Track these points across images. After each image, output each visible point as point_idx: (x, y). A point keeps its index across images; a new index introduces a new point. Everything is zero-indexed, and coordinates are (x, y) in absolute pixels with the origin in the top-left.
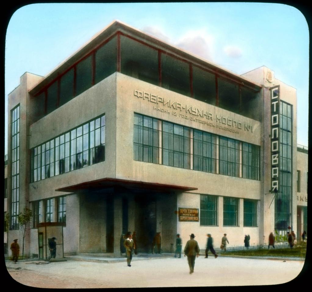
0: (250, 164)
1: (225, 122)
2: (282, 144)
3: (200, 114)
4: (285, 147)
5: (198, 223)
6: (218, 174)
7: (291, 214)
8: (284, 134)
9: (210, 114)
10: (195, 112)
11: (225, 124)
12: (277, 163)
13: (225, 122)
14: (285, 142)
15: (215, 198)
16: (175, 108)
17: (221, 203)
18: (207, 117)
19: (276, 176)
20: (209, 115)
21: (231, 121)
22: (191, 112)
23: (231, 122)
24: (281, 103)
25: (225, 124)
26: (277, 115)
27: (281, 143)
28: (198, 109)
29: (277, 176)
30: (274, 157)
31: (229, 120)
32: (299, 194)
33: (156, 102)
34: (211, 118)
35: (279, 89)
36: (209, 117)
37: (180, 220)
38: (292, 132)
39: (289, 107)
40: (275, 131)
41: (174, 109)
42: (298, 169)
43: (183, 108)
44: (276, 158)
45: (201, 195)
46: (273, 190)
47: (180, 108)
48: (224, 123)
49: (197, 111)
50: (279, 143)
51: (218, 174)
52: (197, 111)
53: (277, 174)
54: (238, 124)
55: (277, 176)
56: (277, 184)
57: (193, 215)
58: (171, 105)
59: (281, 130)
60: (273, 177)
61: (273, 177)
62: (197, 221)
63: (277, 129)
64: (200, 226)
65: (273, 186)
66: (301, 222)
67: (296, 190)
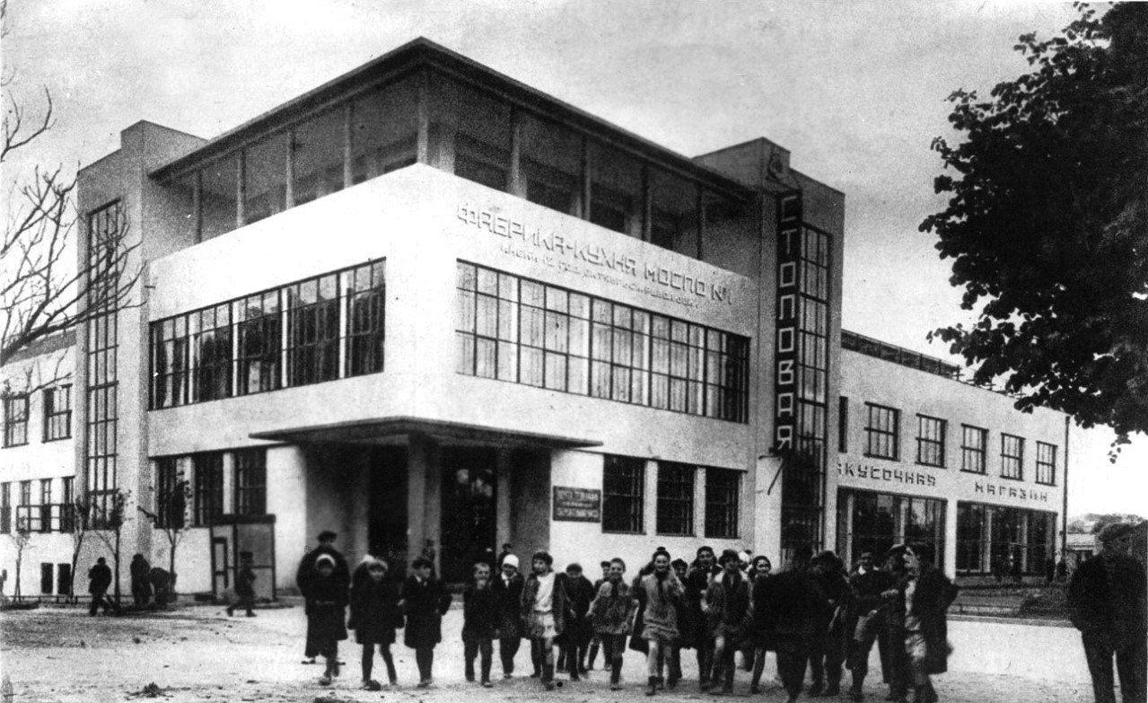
0: (723, 384)
1: (666, 279)
2: (804, 332)
3: (607, 262)
4: (809, 341)
5: (597, 527)
6: (644, 406)
7: (823, 509)
8: (808, 307)
9: (630, 261)
10: (597, 257)
11: (667, 285)
12: (791, 382)
13: (666, 279)
14: (810, 327)
15: (638, 464)
16: (550, 246)
17: (651, 475)
18: (624, 268)
19: (788, 413)
20: (629, 264)
21: (679, 276)
22: (587, 257)
23: (681, 280)
24: (804, 229)
25: (667, 285)
26: (793, 264)
27: (801, 331)
28: (602, 250)
29: (791, 414)
30: (784, 367)
31: (675, 275)
32: (843, 458)
33: (506, 233)
34: (633, 269)
35: (799, 200)
36: (628, 267)
37: (556, 518)
38: (828, 305)
39: (824, 239)
40: (788, 302)
41: (548, 248)
42: (843, 394)
43: (568, 247)
44: (788, 368)
45: (607, 457)
46: (780, 447)
47: (561, 247)
48: (664, 281)
49: (600, 255)
50: (797, 331)
51: (644, 406)
52: (600, 255)
53: (790, 410)
54: (696, 285)
55: (791, 414)
56: (791, 433)
57: (586, 505)
58: (541, 240)
59: (802, 298)
60: (779, 415)
61: (779, 415)
62: (596, 521)
63: (792, 297)
64: (43, 564)
65: (779, 439)
66: (845, 524)
67: (836, 446)
